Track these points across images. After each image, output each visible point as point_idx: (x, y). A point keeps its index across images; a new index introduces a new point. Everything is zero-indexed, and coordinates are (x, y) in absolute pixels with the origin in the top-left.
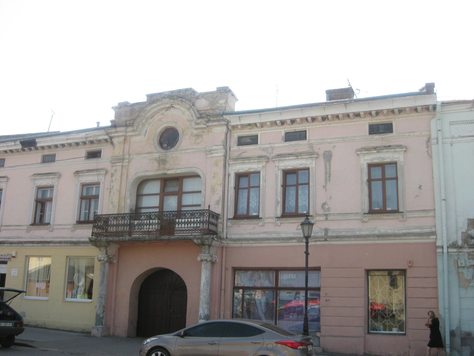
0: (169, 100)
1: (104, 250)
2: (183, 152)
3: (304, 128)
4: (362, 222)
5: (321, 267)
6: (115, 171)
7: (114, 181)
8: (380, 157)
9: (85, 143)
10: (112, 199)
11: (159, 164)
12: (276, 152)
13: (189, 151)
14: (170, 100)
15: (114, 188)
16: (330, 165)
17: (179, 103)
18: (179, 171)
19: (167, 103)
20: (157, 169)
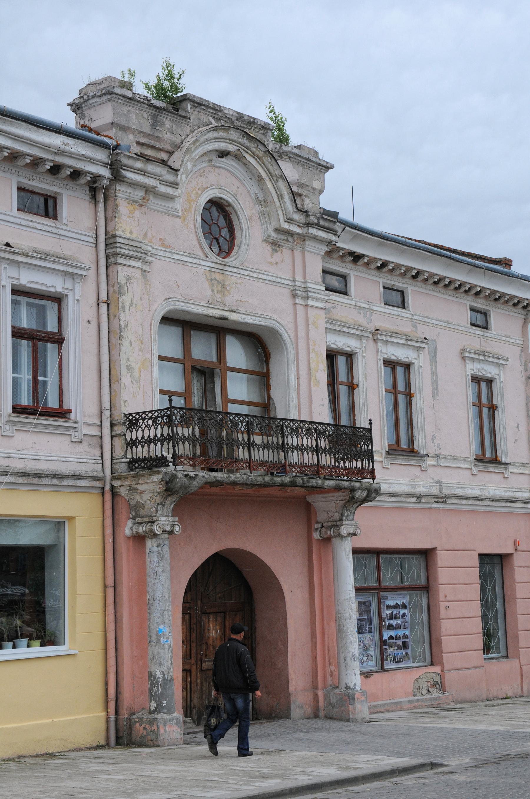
0: (241, 136)
1: (171, 504)
2: (255, 275)
3: (404, 286)
4: (472, 474)
5: (438, 549)
6: (127, 280)
7: (127, 308)
8: (483, 369)
9: (36, 162)
10: (128, 359)
11: (213, 291)
12: (378, 322)
13: (265, 277)
14: (243, 136)
15: (129, 328)
16: (436, 366)
17: (261, 154)
18: (249, 320)
19: (232, 141)
20: (210, 302)
